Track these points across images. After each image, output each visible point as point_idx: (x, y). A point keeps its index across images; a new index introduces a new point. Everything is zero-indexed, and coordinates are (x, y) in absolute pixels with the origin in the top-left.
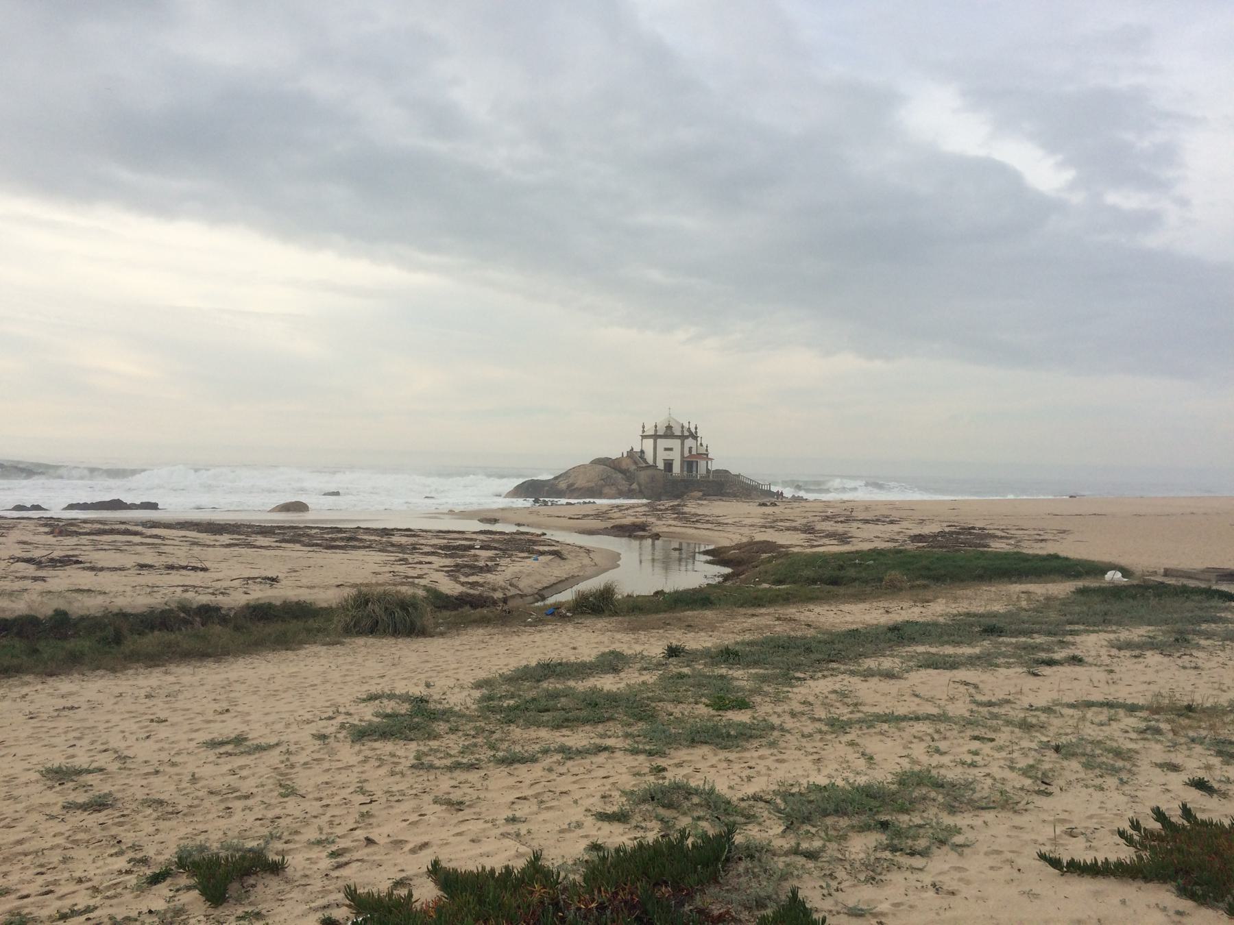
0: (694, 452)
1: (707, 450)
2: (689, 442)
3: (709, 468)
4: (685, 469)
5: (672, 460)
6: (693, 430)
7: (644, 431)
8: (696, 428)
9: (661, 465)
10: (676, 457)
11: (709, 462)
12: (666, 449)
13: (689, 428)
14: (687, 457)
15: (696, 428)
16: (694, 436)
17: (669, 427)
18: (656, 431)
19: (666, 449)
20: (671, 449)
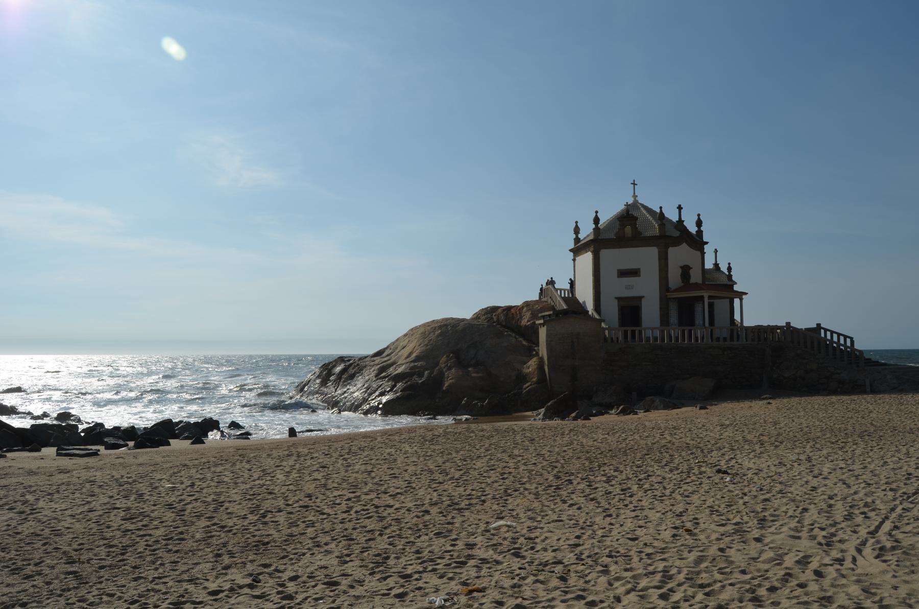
1: (730, 277)
2: (679, 255)
3: (737, 317)
4: (674, 318)
5: (640, 298)
6: (693, 229)
7: (577, 240)
8: (699, 223)
9: (612, 310)
11: (737, 301)
12: (623, 273)
13: (680, 221)
14: (677, 290)
15: (699, 223)
16: (697, 242)
18: (597, 230)
19: (623, 273)
20: (635, 273)
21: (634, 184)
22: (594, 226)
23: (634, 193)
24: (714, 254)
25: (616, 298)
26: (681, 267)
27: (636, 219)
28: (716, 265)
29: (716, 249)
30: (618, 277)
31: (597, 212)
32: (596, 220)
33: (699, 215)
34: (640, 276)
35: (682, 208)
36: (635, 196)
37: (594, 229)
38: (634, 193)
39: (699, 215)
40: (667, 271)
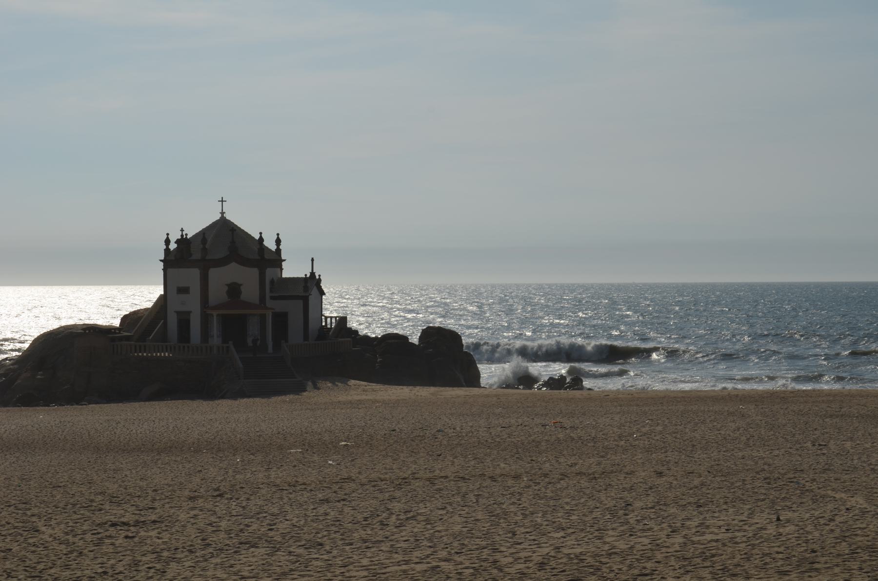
0: (250, 292)
5: (189, 313)
10: (193, 304)
17: (183, 242)
21: (222, 201)
22: (165, 247)
23: (222, 210)
24: (311, 262)
25: (175, 312)
26: (227, 285)
27: (191, 243)
28: (313, 274)
29: (313, 260)
30: (178, 293)
31: (168, 234)
32: (167, 242)
33: (261, 233)
34: (189, 293)
35: (235, 230)
36: (222, 213)
37: (165, 250)
38: (222, 210)
39: (261, 233)
40: (208, 289)
